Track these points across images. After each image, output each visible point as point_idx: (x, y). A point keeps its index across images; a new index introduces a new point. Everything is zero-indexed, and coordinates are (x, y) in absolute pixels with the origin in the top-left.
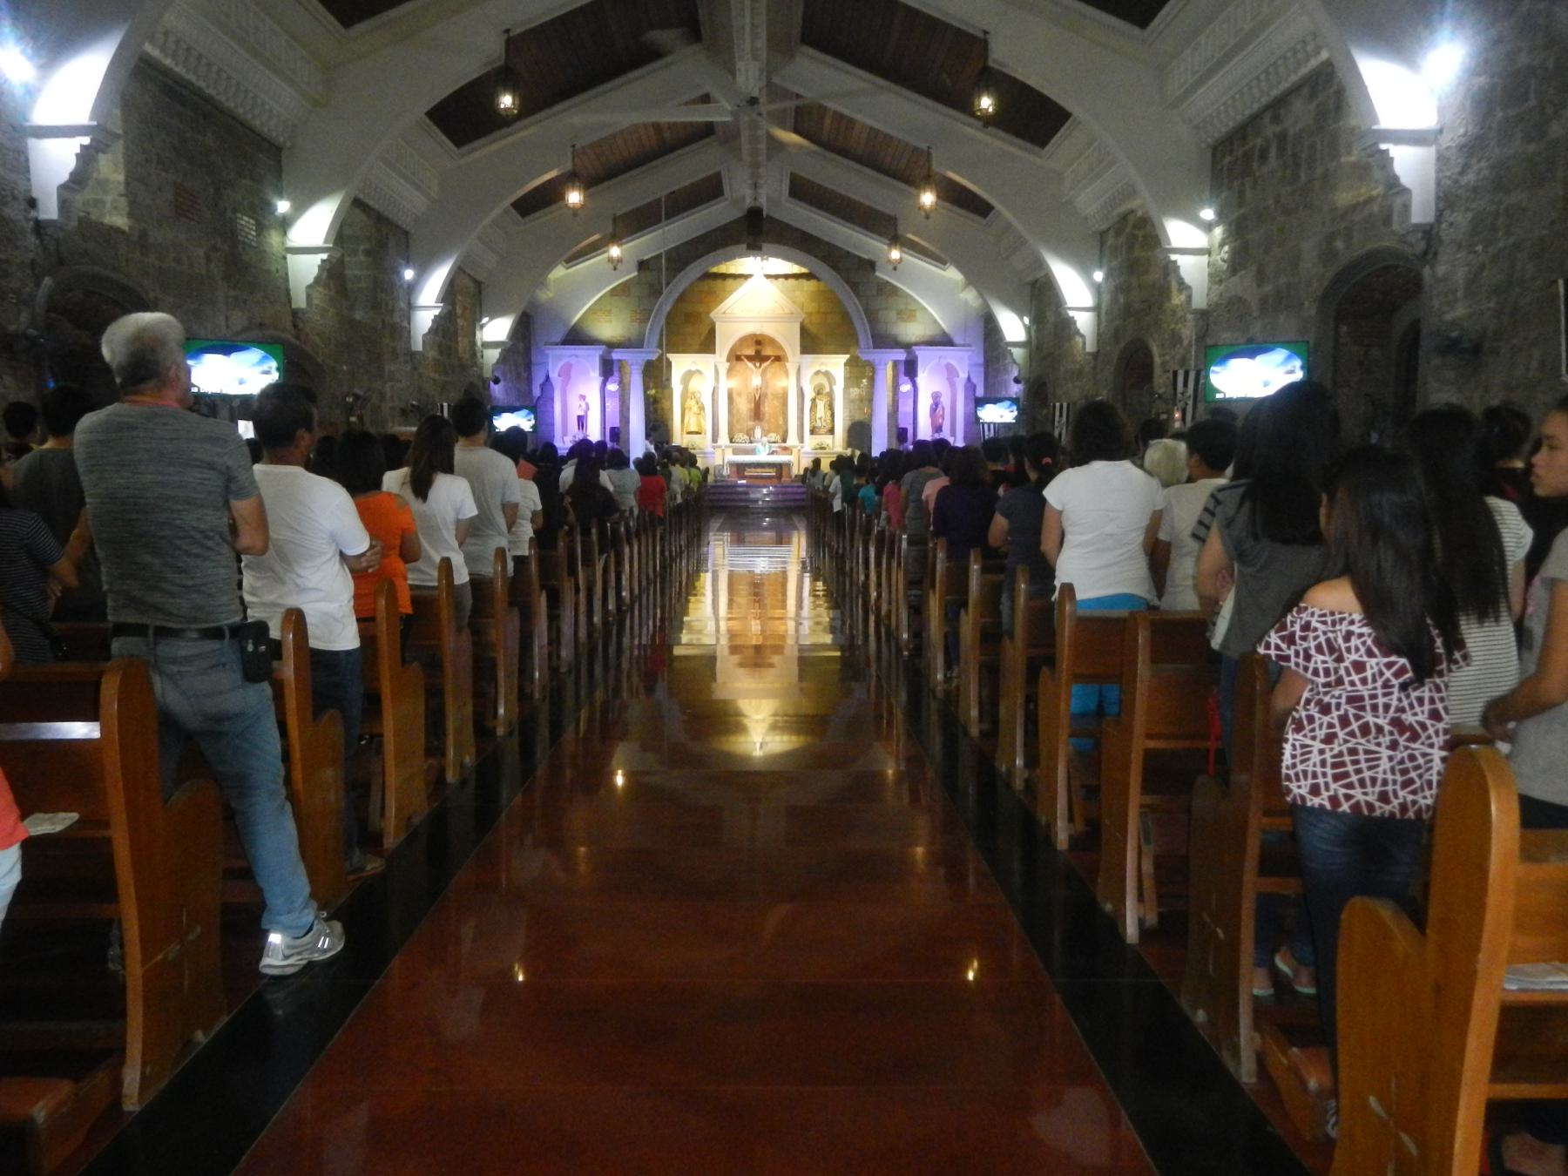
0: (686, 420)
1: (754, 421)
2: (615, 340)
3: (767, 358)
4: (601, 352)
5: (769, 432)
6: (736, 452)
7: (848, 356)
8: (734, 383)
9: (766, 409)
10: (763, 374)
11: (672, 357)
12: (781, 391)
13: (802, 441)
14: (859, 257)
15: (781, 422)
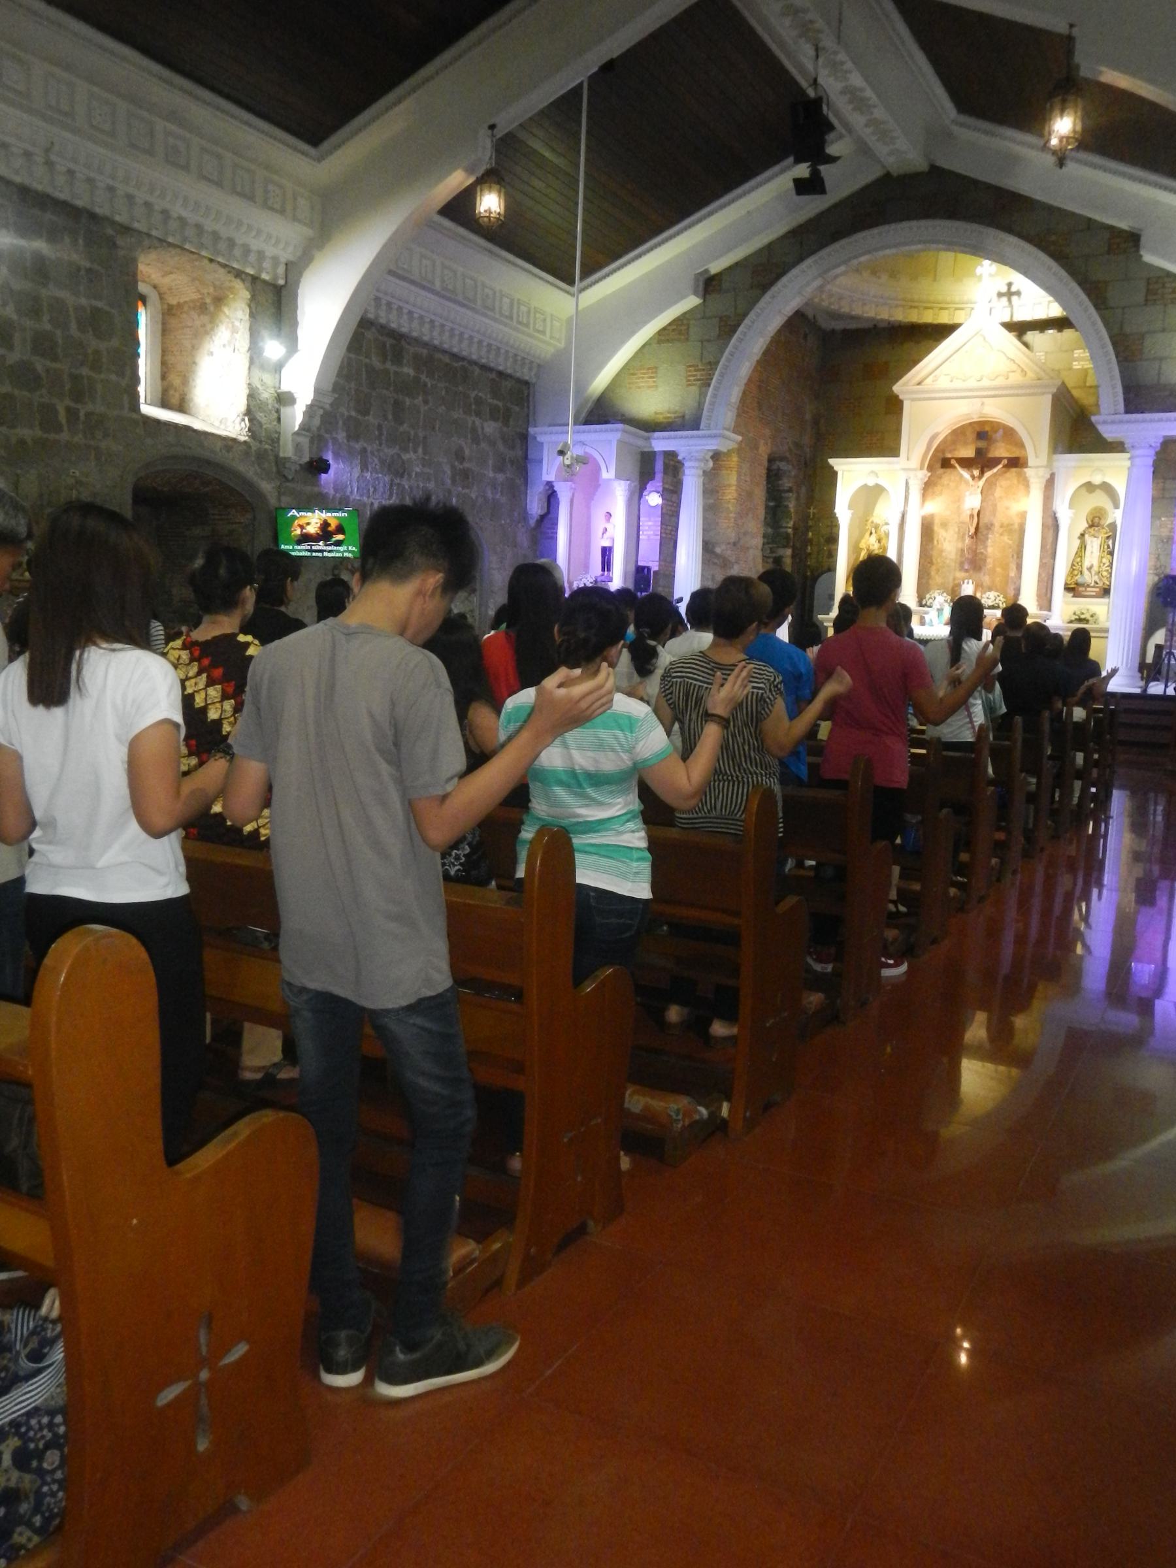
2: (660, 418)
3: (995, 462)
4: (618, 435)
5: (990, 589)
8: (935, 506)
9: (990, 550)
11: (837, 463)
12: (1017, 521)
14: (1111, 228)
15: (1012, 574)
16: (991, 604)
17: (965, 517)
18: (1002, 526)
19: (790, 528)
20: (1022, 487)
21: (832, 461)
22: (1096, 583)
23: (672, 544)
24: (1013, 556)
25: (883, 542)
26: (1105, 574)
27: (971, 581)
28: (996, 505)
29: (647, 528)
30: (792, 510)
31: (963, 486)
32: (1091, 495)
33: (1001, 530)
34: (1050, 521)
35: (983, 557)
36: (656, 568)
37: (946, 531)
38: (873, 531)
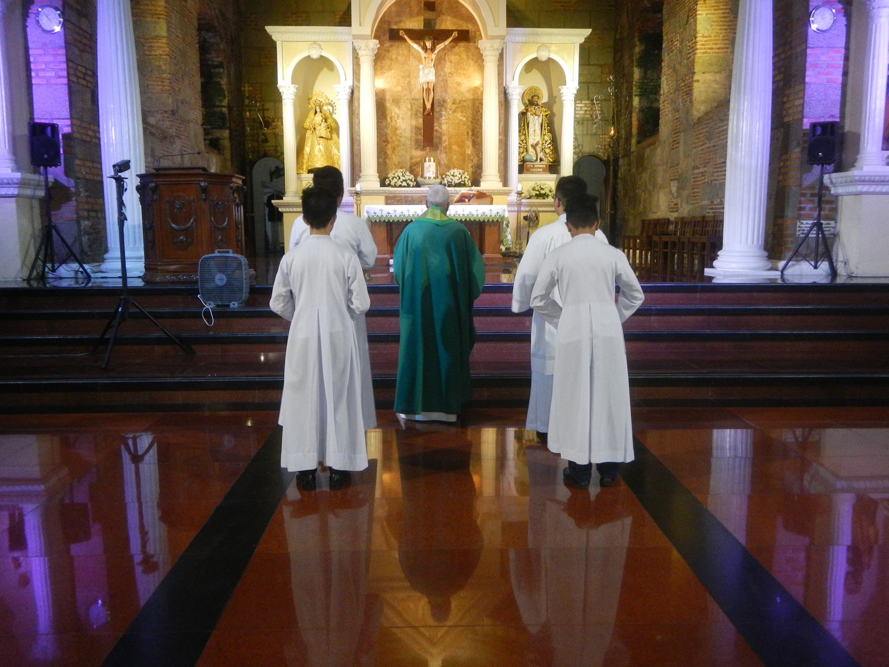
0: (307, 149)
1: (423, 149)
5: (449, 168)
6: (391, 200)
7: (588, 32)
9: (444, 127)
10: (439, 64)
11: (276, 32)
12: (469, 96)
13: (505, 181)
15: (469, 151)
16: (457, 182)
17: (417, 93)
18: (454, 103)
19: (225, 107)
20: (471, 62)
21: (269, 29)
22: (541, 160)
23: (88, 96)
24: (468, 133)
25: (329, 121)
26: (547, 151)
27: (432, 159)
28: (446, 81)
29: (43, 66)
30: (225, 87)
31: (412, 61)
32: (530, 74)
33: (454, 107)
34: (503, 99)
35: (438, 135)
36: (67, 130)
37: (399, 108)
38: (318, 110)
